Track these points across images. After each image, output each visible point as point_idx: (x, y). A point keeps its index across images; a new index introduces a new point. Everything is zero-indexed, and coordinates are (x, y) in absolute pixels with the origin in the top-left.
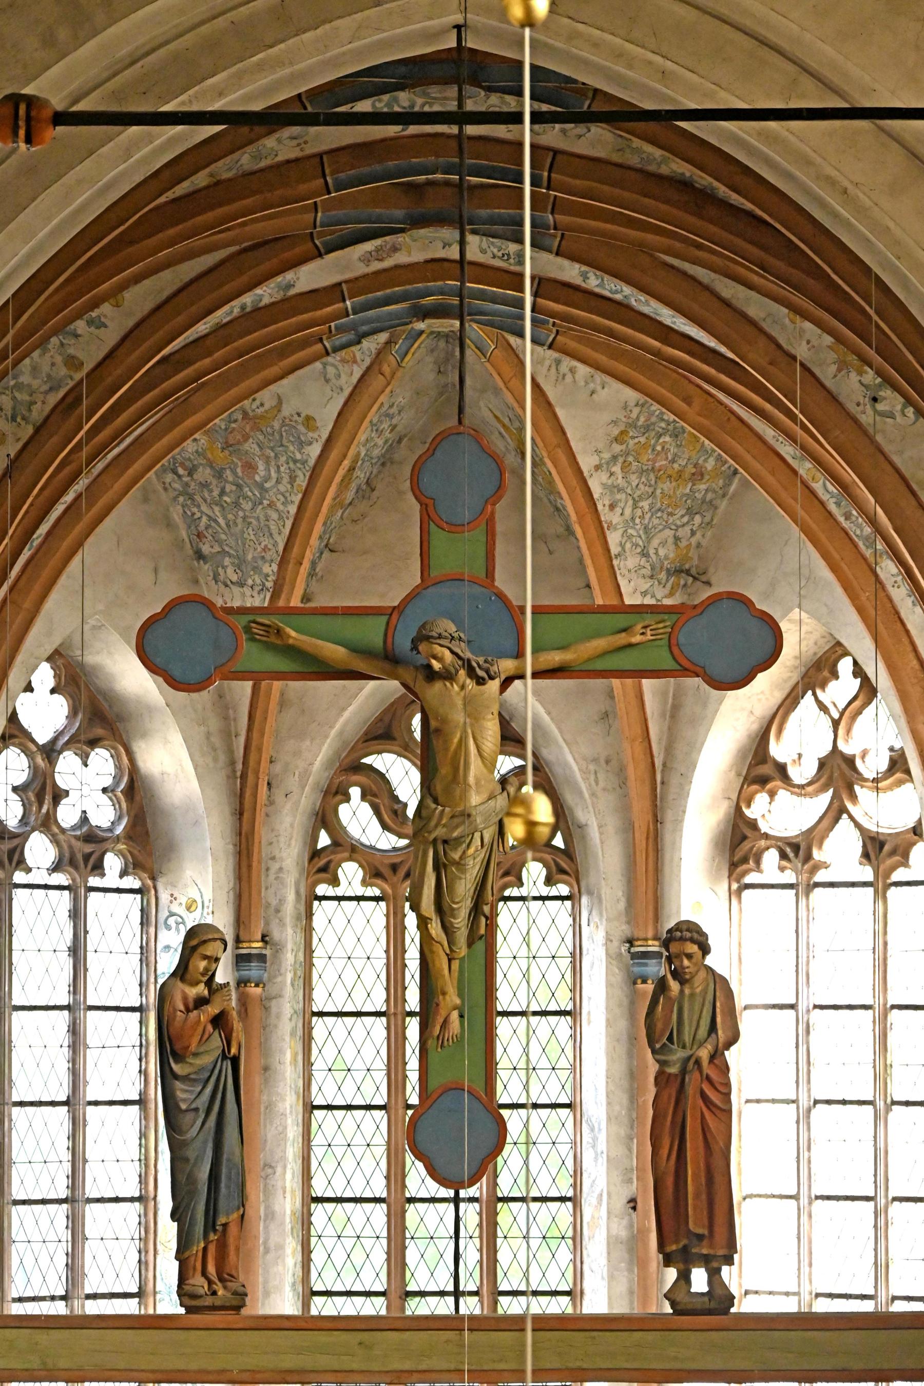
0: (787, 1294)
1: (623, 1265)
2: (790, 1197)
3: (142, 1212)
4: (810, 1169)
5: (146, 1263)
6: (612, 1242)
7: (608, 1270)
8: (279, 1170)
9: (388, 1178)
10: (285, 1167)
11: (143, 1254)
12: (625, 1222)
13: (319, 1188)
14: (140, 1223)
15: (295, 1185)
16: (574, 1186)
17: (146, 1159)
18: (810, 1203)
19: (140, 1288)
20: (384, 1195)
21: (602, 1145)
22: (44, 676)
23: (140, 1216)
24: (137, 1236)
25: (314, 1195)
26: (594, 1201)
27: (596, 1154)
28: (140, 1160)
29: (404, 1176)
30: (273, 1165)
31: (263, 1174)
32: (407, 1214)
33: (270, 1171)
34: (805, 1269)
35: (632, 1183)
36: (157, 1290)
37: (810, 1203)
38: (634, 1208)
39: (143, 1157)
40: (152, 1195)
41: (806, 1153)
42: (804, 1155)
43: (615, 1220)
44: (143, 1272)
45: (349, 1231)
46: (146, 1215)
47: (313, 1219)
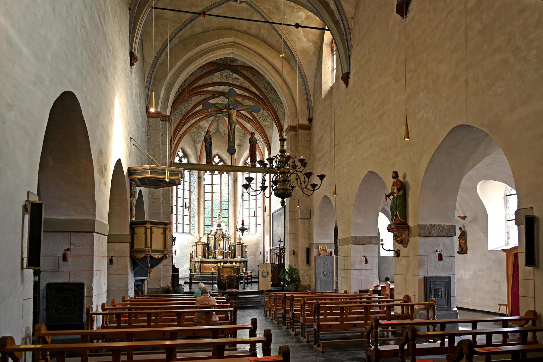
22: (180, 150)
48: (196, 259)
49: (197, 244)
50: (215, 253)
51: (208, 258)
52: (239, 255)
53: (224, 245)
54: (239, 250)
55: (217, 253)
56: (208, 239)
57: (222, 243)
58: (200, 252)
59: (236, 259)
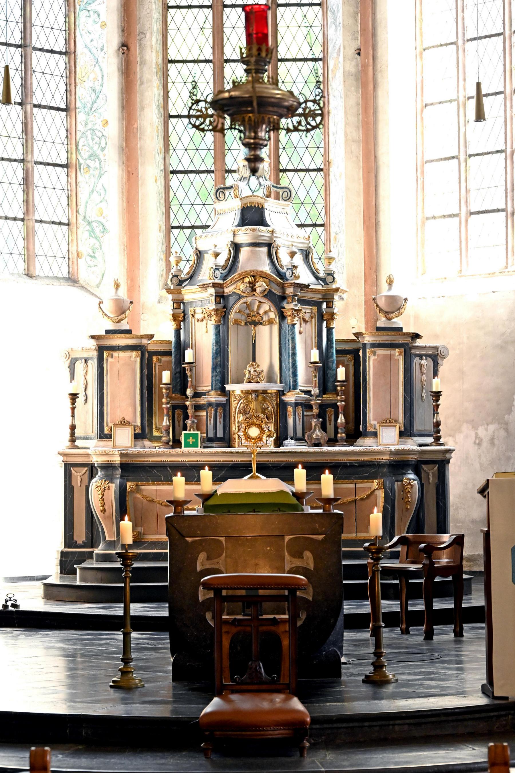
0: (450, 101)
1: (353, 88)
2: (452, 43)
3: (67, 61)
4: (464, 23)
5: (70, 91)
6: (346, 75)
7: (344, 92)
8: (148, 35)
9: (213, 48)
10: (151, 33)
11: (68, 86)
12: (354, 63)
13: (172, 56)
14: (66, 68)
15: (158, 49)
16: (323, 51)
17: (69, 30)
18: (464, 43)
19: (67, 106)
20: (211, 58)
21: (340, 18)
23: (66, 64)
24: (64, 75)
25: (170, 59)
26: (335, 55)
27: (336, 27)
28: (65, 30)
29: (223, 47)
30: (145, 32)
31: (138, 38)
32: (225, 69)
33: (143, 36)
34: (461, 82)
35: (358, 40)
36: (77, 106)
37: (464, 43)
38: (359, 54)
39: (67, 29)
41: (462, 14)
42: (460, 15)
43: (348, 62)
44: (68, 96)
46: (69, 63)
47: (169, 73)
50: (225, 408)
51: (177, 443)
52: (388, 422)
54: (391, 386)
56: (181, 315)
57: (267, 338)
59: (365, 445)
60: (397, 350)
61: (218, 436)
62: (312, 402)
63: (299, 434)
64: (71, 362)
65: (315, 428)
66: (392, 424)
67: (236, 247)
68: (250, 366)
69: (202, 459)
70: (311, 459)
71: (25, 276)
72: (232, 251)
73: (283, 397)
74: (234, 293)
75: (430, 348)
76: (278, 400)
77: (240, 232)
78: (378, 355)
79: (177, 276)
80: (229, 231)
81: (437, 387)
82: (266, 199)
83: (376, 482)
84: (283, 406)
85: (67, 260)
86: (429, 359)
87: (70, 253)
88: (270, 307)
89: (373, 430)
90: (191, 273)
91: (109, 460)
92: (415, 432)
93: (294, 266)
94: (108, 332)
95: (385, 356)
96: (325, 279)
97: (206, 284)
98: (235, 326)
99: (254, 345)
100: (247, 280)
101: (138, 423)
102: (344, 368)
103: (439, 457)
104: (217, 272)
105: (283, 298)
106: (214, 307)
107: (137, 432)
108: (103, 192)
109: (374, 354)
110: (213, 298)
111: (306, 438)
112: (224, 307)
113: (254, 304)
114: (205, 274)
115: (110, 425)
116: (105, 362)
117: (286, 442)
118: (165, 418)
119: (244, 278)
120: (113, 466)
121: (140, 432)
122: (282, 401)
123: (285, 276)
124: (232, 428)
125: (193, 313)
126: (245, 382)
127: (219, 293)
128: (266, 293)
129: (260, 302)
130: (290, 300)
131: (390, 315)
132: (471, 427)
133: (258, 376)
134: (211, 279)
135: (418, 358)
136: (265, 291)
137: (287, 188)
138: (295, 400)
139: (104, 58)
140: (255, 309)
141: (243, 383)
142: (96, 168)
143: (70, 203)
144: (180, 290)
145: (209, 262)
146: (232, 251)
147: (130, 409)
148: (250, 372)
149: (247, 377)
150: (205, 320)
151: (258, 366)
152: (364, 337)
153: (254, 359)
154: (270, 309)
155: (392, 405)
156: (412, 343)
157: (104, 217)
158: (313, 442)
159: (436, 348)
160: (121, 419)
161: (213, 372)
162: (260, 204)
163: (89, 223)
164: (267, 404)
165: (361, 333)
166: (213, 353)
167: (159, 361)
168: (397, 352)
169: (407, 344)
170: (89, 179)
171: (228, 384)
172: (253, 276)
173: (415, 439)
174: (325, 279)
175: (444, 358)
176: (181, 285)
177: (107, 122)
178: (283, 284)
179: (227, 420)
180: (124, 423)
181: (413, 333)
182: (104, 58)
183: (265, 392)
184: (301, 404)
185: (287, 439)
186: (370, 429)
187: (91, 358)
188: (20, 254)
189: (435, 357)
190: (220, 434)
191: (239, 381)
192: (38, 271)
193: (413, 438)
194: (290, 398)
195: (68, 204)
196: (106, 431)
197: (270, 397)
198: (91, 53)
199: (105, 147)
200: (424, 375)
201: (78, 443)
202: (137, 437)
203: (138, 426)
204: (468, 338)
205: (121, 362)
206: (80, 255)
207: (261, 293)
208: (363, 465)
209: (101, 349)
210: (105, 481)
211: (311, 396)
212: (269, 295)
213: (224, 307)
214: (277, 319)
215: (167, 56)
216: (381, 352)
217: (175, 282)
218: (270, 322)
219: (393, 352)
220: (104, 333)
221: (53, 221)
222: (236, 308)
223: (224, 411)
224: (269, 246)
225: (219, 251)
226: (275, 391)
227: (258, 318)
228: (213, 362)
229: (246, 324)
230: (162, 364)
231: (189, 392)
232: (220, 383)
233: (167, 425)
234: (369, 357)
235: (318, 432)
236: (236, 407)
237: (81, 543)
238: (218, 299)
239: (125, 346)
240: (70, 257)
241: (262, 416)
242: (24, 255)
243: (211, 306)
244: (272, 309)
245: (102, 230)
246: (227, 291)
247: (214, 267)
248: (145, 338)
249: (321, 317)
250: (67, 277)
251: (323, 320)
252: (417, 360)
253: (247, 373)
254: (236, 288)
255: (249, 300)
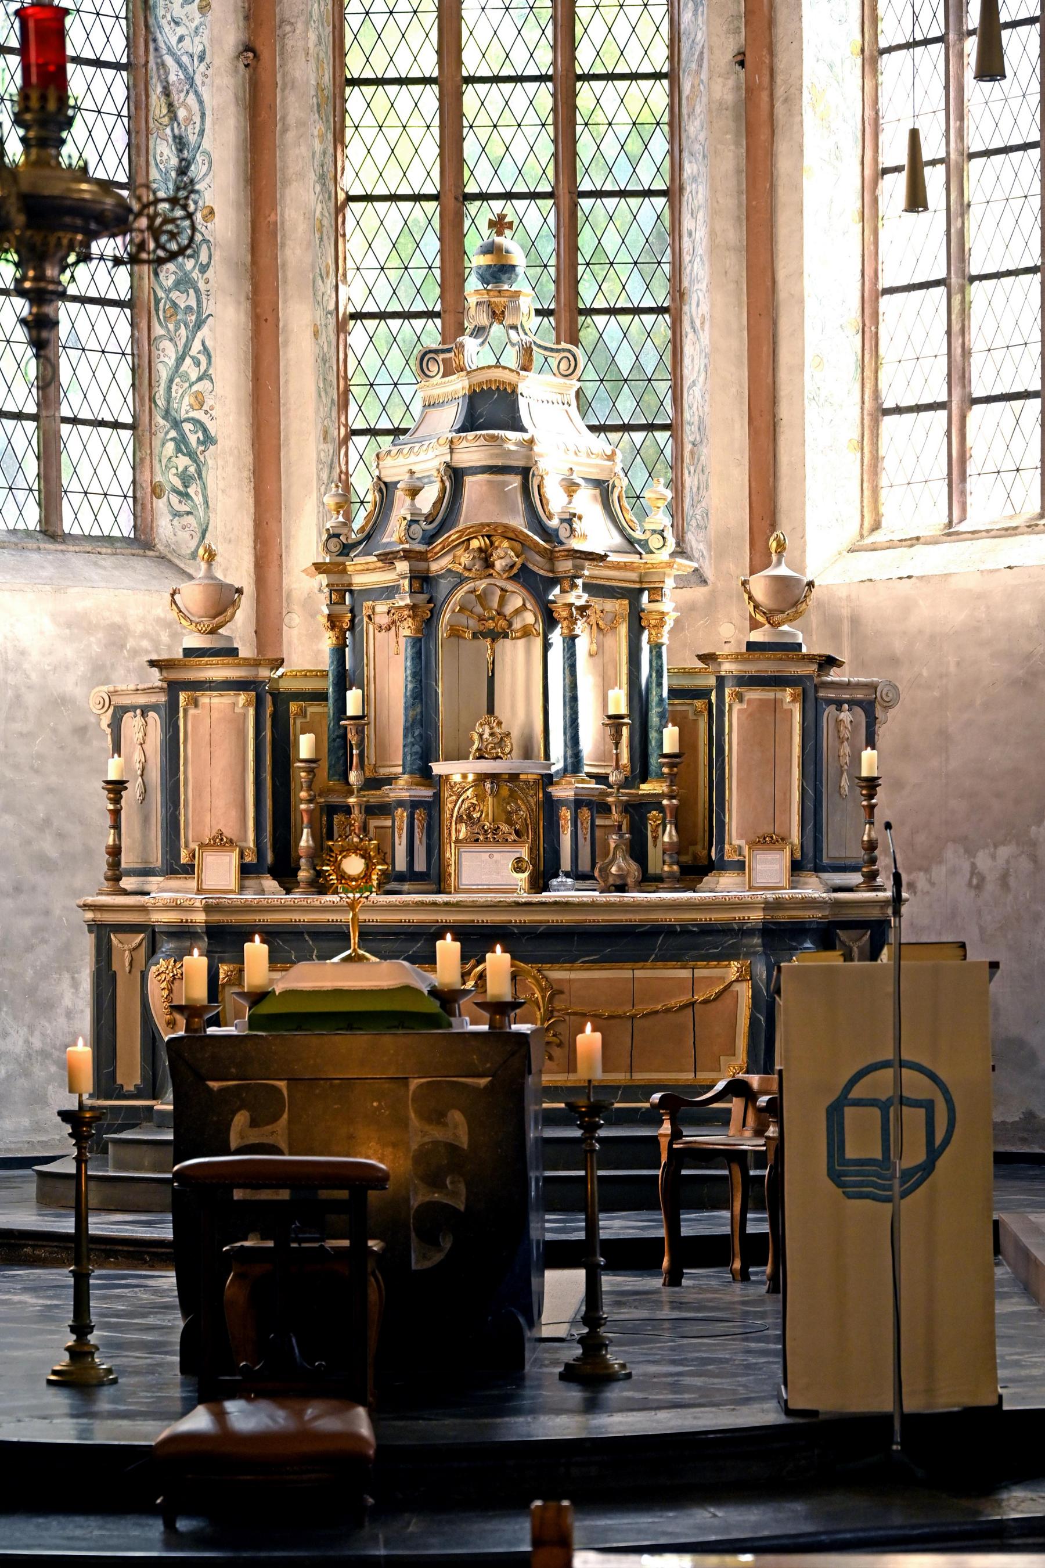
1: (729, 136)
5: (138, 147)
8: (300, 27)
12: (731, 83)
15: (322, 55)
16: (671, 58)
24: (125, 112)
28: (126, 18)
29: (460, 50)
30: (293, 20)
32: (465, 98)
33: (288, 28)
40: (142, 61)
43: (720, 80)
44: (133, 158)
45: (393, 119)
46: (135, 86)
48: (166, 898)
49: (177, 685)
50: (429, 812)
53: (562, 697)
54: (774, 765)
55: (453, 808)
56: (346, 618)
58: (221, 794)
59: (723, 886)
60: (789, 690)
61: (417, 868)
62: (610, 799)
63: (584, 865)
64: (114, 715)
65: (614, 854)
66: (777, 846)
67: (456, 475)
68: (481, 725)
69: (375, 918)
70: (600, 918)
71: (40, 536)
72: (447, 484)
73: (550, 789)
74: (449, 570)
75: (859, 685)
76: (541, 795)
77: (464, 444)
78: (749, 701)
79: (338, 536)
80: (442, 441)
81: (871, 767)
82: (522, 373)
83: (735, 965)
84: (551, 806)
85: (130, 501)
86: (858, 710)
87: (138, 486)
88: (524, 601)
89: (736, 858)
90: (367, 529)
91: (184, 918)
92: (825, 861)
93: (574, 515)
94: (188, 652)
95: (762, 702)
96: (647, 541)
97: (392, 553)
98: (454, 640)
99: (491, 680)
100: (475, 544)
101: (252, 845)
102: (676, 729)
103: (875, 914)
104: (414, 527)
105: (553, 582)
106: (408, 601)
107: (247, 860)
108: (203, 359)
109: (740, 698)
110: (406, 582)
111: (596, 874)
112: (430, 601)
113: (493, 593)
114: (394, 534)
115: (194, 846)
116: (181, 714)
117: (554, 882)
118: (305, 831)
119: (468, 540)
120: (191, 930)
121: (255, 861)
122: (548, 796)
123: (557, 536)
124: (445, 852)
125: (370, 612)
126: (471, 758)
127: (419, 571)
128: (515, 571)
129: (502, 590)
130: (566, 584)
131: (779, 617)
132: (962, 851)
133: (501, 743)
134: (401, 543)
135: (833, 707)
136: (512, 567)
137: (569, 351)
138: (576, 795)
139: (205, 76)
140: (495, 605)
141: (467, 759)
142: (189, 309)
143: (137, 382)
144: (344, 564)
145: (401, 508)
146: (447, 484)
147: (234, 813)
148: (481, 735)
149: (475, 747)
150: (393, 628)
151: (500, 724)
152: (720, 664)
153: (491, 710)
154: (524, 605)
155: (776, 805)
156: (819, 676)
157: (206, 412)
158: (611, 881)
159: (873, 687)
160: (214, 833)
161: (405, 736)
162: (510, 384)
163: (176, 424)
164: (516, 804)
165: (714, 654)
166: (406, 696)
167: (303, 713)
168: (787, 694)
169: (809, 677)
170: (176, 330)
171: (438, 760)
172: (489, 537)
173: (825, 876)
174: (647, 541)
175: (890, 707)
176: (347, 555)
177: (212, 212)
178: (552, 552)
179: (436, 834)
180: (220, 843)
181: (820, 656)
182: (205, 76)
183: (514, 777)
184: (589, 804)
185: (557, 876)
186: (730, 856)
187: (154, 708)
188: (31, 490)
189: (869, 705)
190: (420, 866)
191: (460, 755)
192: (68, 525)
193: (820, 874)
194: (564, 792)
195: (133, 385)
196: (184, 859)
197: (522, 789)
198: (180, 65)
199: (208, 265)
200: (846, 743)
201: (127, 883)
202: (246, 870)
203: (249, 849)
204: (958, 664)
205: (215, 715)
206: (158, 490)
207: (505, 571)
208: (708, 930)
209: (173, 688)
210: (175, 962)
211: (610, 787)
212: (522, 575)
213: (430, 601)
214: (540, 627)
215: (343, 72)
216: (754, 694)
217: (333, 549)
218: (526, 632)
219: (779, 695)
220: (180, 655)
221: (100, 418)
222: (455, 603)
223: (430, 816)
224: (525, 472)
225: (419, 484)
226: (535, 777)
227: (503, 623)
228: (406, 715)
229: (475, 636)
230: (308, 720)
231: (353, 777)
232: (421, 758)
233: (308, 847)
234: (730, 706)
235: (620, 860)
236: (453, 809)
237: (132, 1089)
238: (416, 585)
239: (223, 682)
240: (138, 495)
241: (505, 828)
242: (39, 491)
243: (402, 599)
244: (528, 605)
245: (201, 438)
246: (435, 567)
247: (409, 518)
248: (265, 666)
249: (637, 623)
250: (132, 536)
251: (642, 629)
252: (830, 710)
253: (476, 737)
254: (454, 562)
255: (482, 585)
